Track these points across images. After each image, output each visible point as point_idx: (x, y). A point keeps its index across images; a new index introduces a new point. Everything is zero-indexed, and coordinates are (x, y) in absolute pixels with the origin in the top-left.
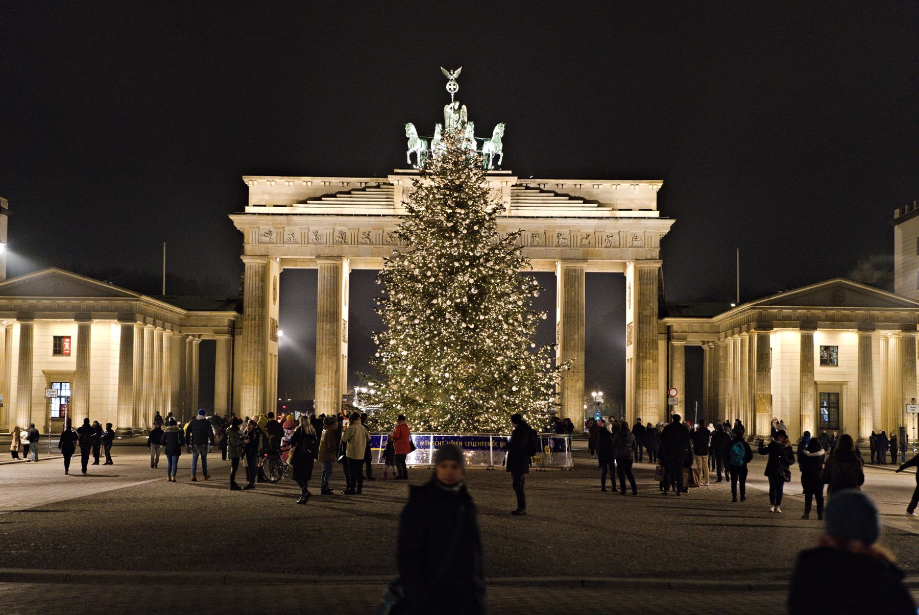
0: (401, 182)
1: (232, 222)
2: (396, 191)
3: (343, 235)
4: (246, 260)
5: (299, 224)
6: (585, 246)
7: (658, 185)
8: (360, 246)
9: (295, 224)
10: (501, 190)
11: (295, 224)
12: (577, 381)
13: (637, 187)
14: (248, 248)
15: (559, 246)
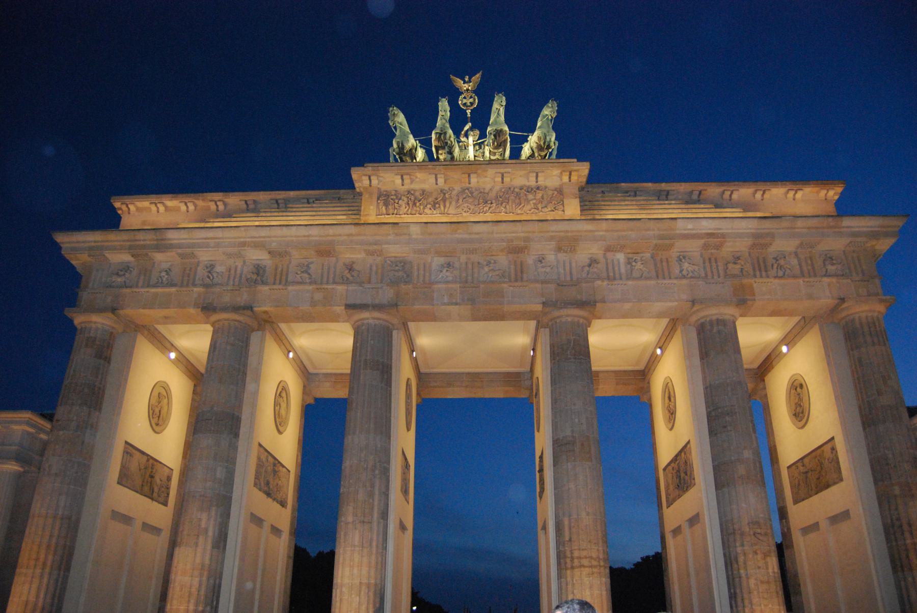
0: (375, 182)
1: (57, 247)
2: (365, 197)
3: (259, 270)
4: (79, 320)
5: (179, 246)
6: (734, 276)
7: (833, 193)
8: (290, 288)
9: (170, 247)
10: (560, 191)
11: (170, 247)
12: (766, 555)
13: (799, 195)
14: (84, 296)
15: (684, 277)
